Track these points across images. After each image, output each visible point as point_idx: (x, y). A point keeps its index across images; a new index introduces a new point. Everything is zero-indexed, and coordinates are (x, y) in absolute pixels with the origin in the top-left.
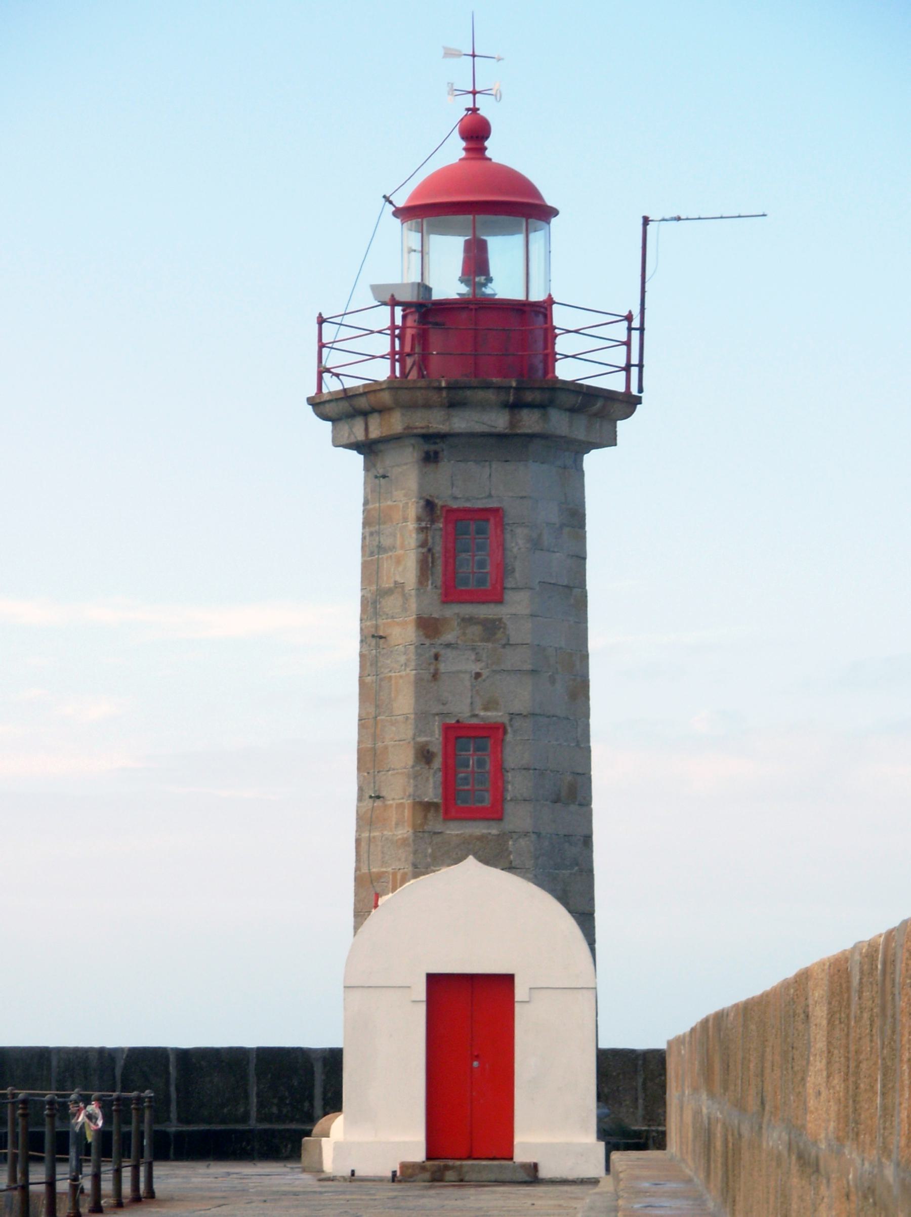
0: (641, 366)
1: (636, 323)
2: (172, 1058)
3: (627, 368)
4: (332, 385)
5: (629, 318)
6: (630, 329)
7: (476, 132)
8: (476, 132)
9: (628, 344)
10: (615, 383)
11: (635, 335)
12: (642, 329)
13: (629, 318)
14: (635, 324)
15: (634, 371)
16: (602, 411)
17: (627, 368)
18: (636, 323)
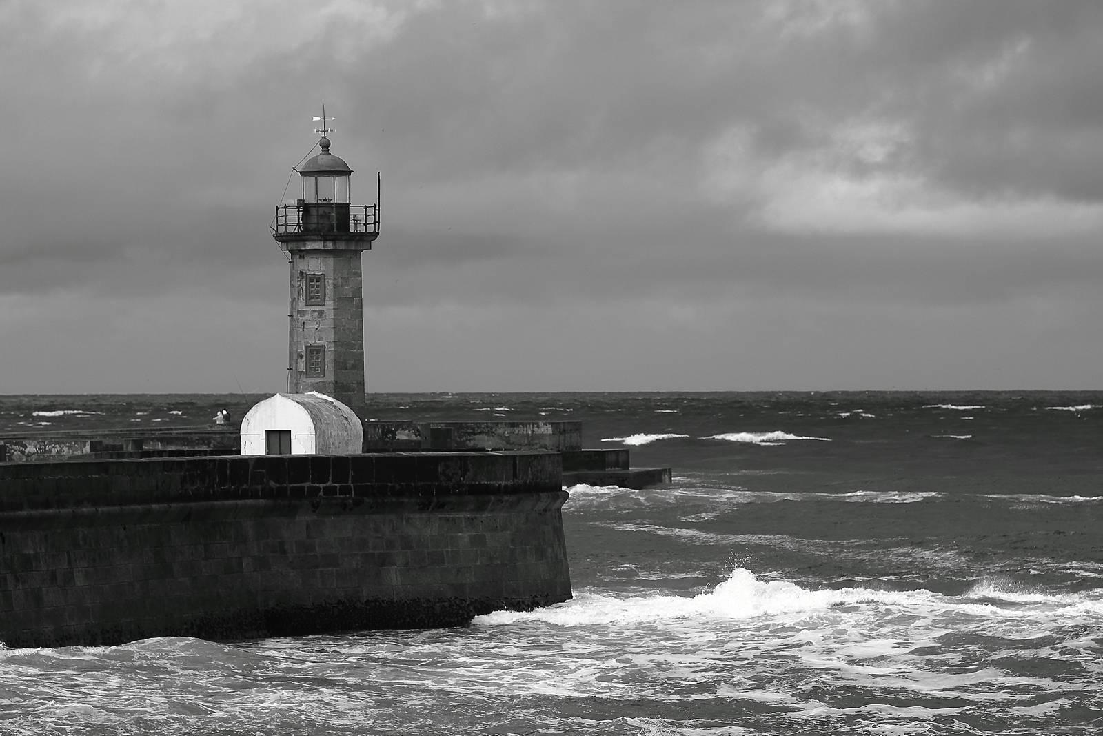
0: (379, 222)
1: (377, 208)
2: (251, 463)
3: (374, 223)
4: (281, 230)
5: (375, 206)
6: (375, 210)
7: (326, 146)
8: (326, 146)
9: (375, 215)
10: (370, 229)
11: (377, 212)
12: (379, 210)
13: (375, 206)
14: (377, 208)
15: (377, 224)
16: (366, 239)
17: (374, 223)
18: (377, 208)
